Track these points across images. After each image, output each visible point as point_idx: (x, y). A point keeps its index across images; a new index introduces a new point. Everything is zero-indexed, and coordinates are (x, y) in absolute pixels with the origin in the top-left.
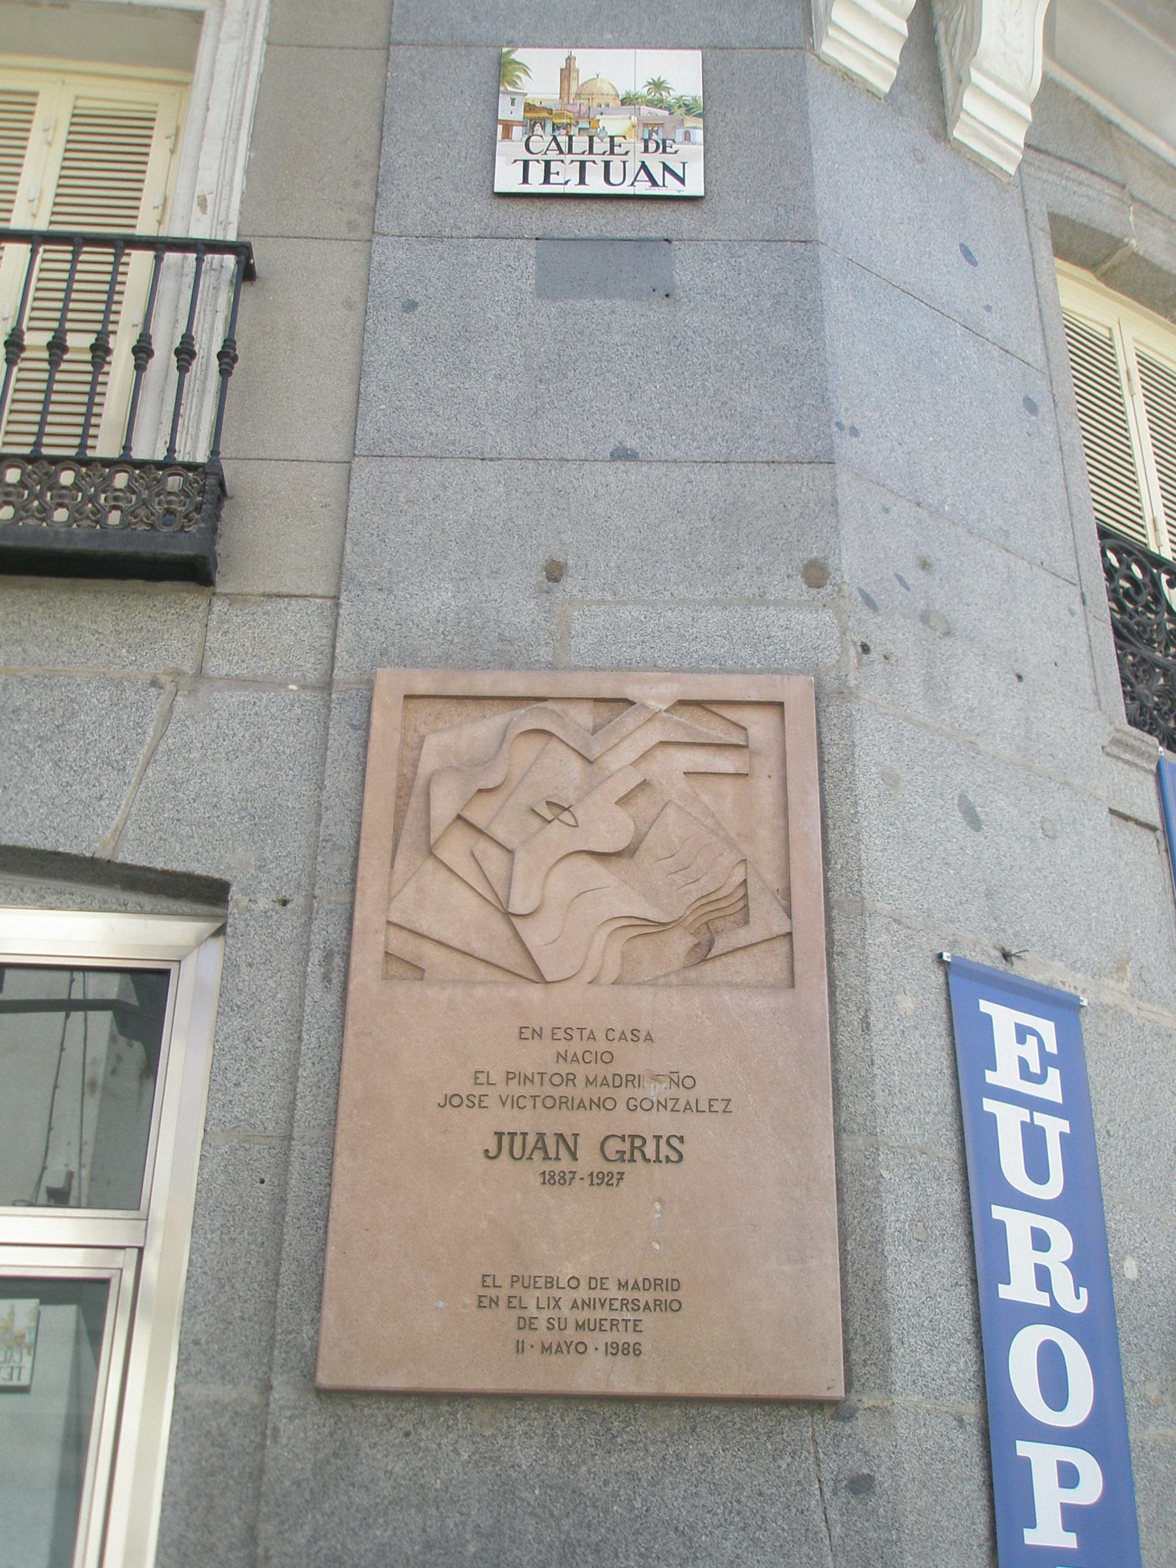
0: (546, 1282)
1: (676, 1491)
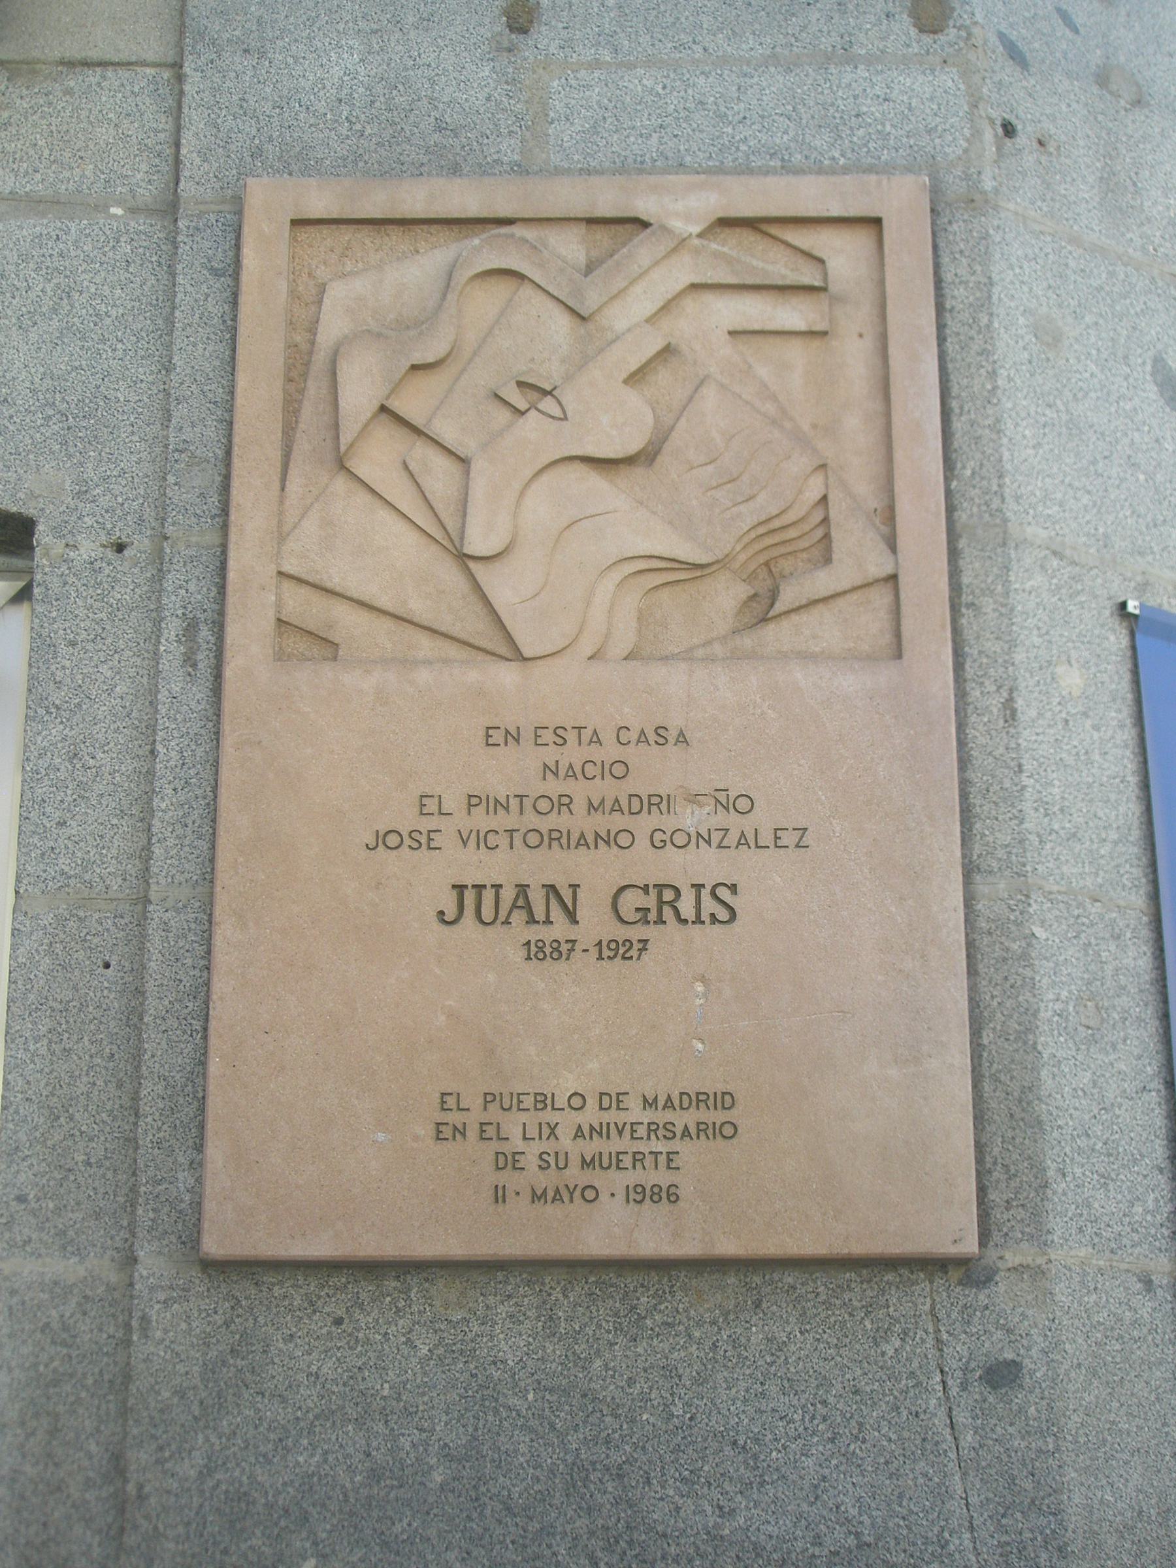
0: (536, 1101)
1: (734, 1390)
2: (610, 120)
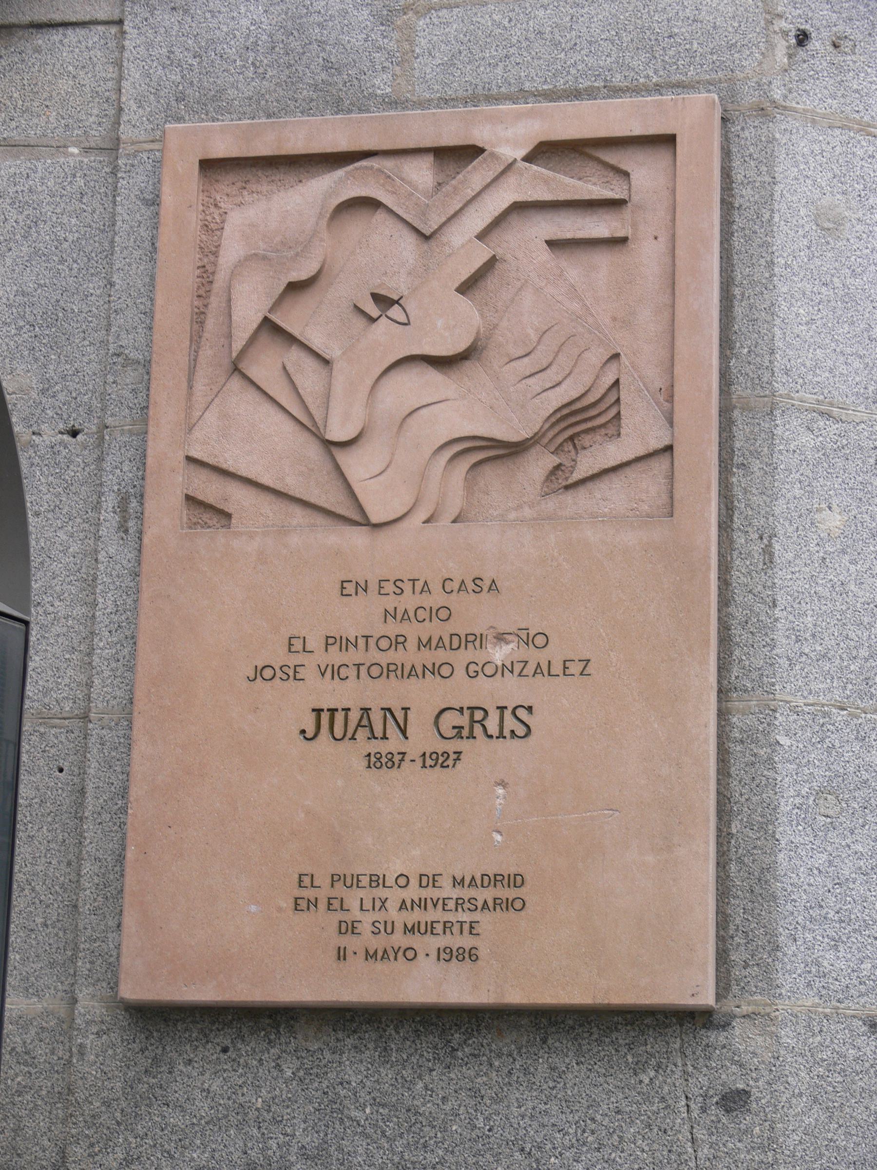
0: (371, 880)
1: (523, 1109)
2: (465, 52)
